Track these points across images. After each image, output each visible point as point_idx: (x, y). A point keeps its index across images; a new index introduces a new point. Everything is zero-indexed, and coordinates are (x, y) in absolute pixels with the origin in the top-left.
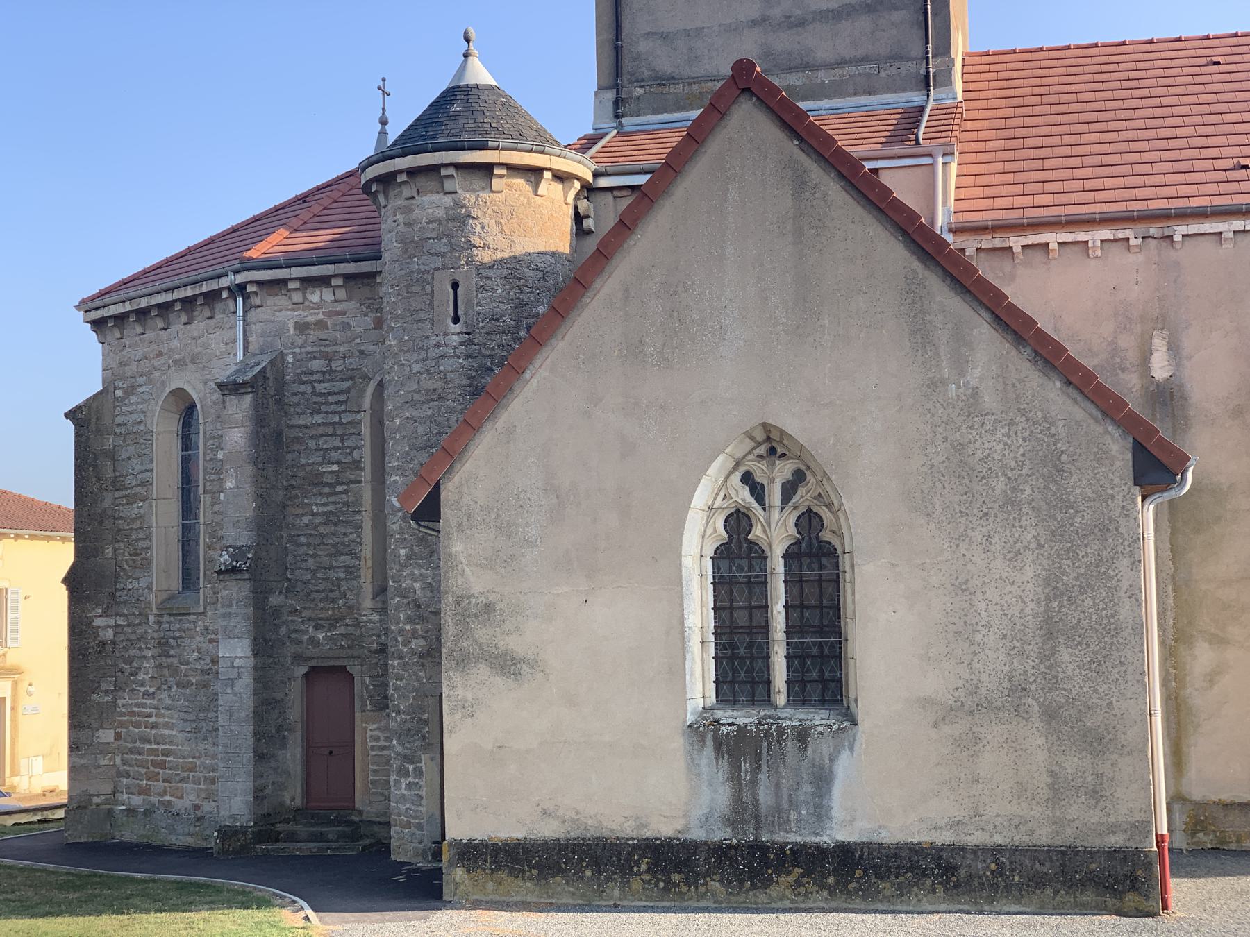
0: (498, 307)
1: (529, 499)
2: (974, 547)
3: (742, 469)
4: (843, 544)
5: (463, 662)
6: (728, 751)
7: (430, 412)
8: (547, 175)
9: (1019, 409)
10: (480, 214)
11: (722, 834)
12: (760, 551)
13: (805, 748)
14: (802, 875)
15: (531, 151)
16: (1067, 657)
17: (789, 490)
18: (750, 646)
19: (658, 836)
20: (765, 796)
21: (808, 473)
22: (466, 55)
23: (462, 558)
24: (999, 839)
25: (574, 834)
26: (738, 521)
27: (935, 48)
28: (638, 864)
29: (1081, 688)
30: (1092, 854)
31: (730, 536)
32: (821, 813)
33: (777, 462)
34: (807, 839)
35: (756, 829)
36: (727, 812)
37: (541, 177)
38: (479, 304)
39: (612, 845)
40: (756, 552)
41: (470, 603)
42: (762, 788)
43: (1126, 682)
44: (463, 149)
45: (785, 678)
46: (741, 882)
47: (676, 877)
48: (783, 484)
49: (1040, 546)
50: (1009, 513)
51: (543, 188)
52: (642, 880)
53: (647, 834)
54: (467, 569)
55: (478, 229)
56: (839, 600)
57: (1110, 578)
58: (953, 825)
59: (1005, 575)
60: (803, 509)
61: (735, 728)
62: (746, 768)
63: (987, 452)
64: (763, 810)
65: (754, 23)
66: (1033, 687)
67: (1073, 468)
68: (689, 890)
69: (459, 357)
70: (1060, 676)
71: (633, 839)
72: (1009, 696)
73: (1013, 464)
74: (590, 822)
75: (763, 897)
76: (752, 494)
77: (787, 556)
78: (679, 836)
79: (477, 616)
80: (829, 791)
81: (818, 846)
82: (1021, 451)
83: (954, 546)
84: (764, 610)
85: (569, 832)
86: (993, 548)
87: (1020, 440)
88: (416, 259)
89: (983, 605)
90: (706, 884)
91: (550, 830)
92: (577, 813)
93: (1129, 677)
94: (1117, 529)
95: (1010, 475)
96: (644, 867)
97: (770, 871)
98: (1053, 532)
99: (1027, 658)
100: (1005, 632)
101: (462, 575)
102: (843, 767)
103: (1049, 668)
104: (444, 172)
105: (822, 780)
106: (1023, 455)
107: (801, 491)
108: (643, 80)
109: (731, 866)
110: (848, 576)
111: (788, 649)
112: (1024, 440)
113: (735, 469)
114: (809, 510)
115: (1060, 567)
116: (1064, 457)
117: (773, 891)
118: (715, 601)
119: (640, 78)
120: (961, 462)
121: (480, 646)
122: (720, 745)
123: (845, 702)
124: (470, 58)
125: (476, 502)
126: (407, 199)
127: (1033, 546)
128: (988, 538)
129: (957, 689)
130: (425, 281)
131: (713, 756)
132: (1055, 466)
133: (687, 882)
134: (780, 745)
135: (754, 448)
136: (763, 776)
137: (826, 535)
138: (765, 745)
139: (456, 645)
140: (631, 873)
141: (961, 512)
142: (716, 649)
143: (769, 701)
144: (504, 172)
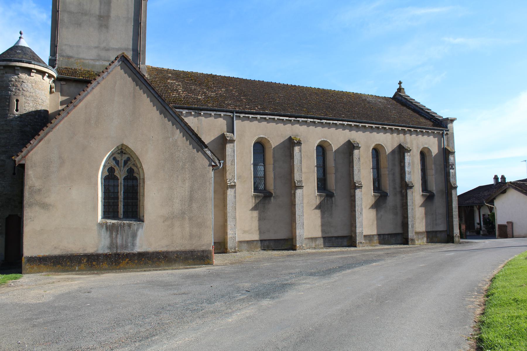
0: (30, 108)
1: (54, 160)
2: (174, 178)
3: (114, 156)
4: (140, 177)
5: (31, 205)
6: (109, 230)
7: (6, 136)
8: (47, 74)
9: (186, 146)
10: (26, 82)
11: (107, 251)
12: (117, 178)
13: (130, 229)
14: (129, 261)
15: (44, 67)
16: (195, 206)
17: (126, 163)
18: (114, 202)
19: (89, 253)
20: (119, 241)
21: (131, 158)
22: (20, 38)
23: (32, 176)
24: (177, 249)
25: (64, 253)
26: (111, 170)
27: (142, 62)
28: (83, 260)
29: (197, 212)
30: (198, 251)
31: (109, 174)
32: (133, 245)
33: (123, 155)
34: (130, 252)
35: (116, 249)
36: (109, 245)
37: (45, 75)
38: (25, 107)
39: (75, 256)
40: (116, 178)
41: (34, 188)
42: (118, 239)
43: (207, 211)
44: (23, 62)
45: (123, 211)
46: (112, 264)
47: (94, 263)
48: (125, 161)
49: (190, 179)
50: (182, 170)
51: (45, 78)
52: (84, 264)
53: (86, 252)
54: (33, 179)
55: (26, 86)
56: (138, 191)
57: (205, 187)
58: (167, 246)
59: (181, 185)
60: (129, 167)
61: (112, 223)
62: (114, 234)
63: (178, 156)
65: (96, 47)
66: (187, 212)
67: (197, 161)
68: (98, 266)
69: (17, 121)
70: (193, 210)
71: (81, 254)
72: (181, 214)
73: (184, 159)
74: (69, 250)
75: (118, 267)
76: (116, 163)
77: (124, 179)
78: (95, 252)
79: (36, 192)
80: (136, 240)
81: (133, 254)
82: (186, 156)
83: (170, 178)
84: (117, 193)
85: (63, 253)
86: (179, 179)
87: (186, 153)
88: (4, 92)
89: (176, 193)
90: (102, 264)
92: (65, 247)
93: (208, 210)
94: (206, 175)
95: (183, 161)
96: (85, 261)
97: (120, 260)
98: (193, 176)
99: (186, 205)
100: (181, 199)
101: (32, 180)
102: (140, 233)
103: (190, 208)
104: (16, 68)
106: (186, 157)
107: (129, 163)
108: (64, 56)
109: (110, 259)
110: (141, 185)
111: (124, 203)
112: (187, 153)
113: (112, 156)
114: (131, 168)
115: (194, 184)
116: (196, 158)
117: (121, 265)
118: (104, 190)
119: (63, 55)
120: (172, 157)
121: (36, 201)
122: (107, 228)
123: (138, 217)
124: (22, 39)
125: (37, 160)
126: (2, 74)
127: (188, 179)
128: (178, 176)
129: (169, 213)
130: (7, 98)
131: (105, 231)
132: (194, 160)
133: (97, 264)
134: (124, 228)
135: (118, 151)
137: (135, 175)
138: (120, 228)
139: (29, 200)
140: (81, 263)
141: (171, 170)
142: (104, 203)
143: (118, 217)
144: (35, 71)
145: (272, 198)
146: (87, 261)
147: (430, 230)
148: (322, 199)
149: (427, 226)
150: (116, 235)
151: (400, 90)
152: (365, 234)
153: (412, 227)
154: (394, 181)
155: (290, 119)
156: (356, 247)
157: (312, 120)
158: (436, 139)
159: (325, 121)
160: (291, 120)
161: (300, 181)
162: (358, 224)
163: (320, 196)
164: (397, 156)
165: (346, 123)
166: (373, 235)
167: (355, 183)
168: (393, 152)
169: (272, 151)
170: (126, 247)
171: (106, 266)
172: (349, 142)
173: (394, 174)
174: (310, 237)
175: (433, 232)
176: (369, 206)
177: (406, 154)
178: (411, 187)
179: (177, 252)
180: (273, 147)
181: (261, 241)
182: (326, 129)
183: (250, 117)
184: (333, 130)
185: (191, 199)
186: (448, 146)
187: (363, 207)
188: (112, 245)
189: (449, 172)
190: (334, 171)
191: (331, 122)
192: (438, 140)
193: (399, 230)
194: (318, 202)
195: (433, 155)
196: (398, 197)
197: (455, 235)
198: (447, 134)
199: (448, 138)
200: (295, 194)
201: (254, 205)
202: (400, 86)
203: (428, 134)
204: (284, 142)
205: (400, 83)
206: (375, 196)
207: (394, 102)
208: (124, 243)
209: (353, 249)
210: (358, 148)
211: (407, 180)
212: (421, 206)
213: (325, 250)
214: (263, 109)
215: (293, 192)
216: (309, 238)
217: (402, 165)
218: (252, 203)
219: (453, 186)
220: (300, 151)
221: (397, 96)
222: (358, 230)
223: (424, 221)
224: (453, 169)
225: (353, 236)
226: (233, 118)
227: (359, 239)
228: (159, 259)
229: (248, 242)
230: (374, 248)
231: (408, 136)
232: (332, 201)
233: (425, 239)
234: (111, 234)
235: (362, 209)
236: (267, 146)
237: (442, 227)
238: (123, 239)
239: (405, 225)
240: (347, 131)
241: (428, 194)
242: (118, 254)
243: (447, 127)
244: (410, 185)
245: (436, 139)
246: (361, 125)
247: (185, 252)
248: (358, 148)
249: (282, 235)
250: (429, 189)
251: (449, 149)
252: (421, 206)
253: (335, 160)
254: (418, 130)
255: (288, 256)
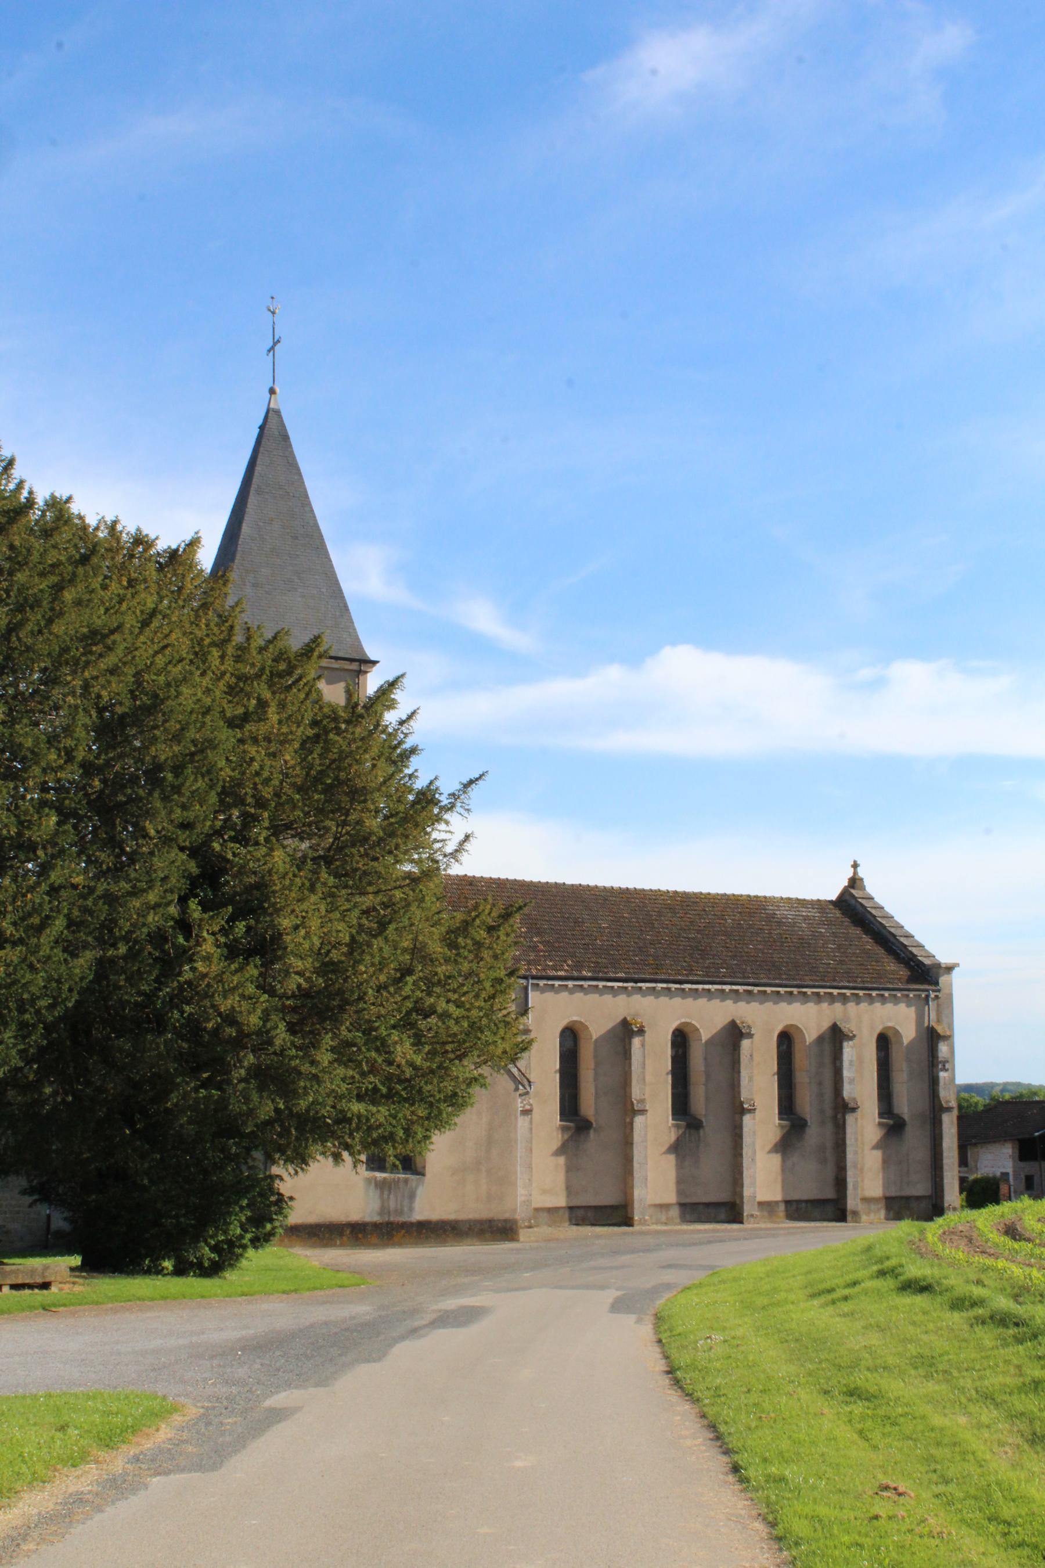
11: (376, 1219)
20: (392, 1204)
24: (471, 1216)
30: (499, 1220)
32: (411, 1209)
47: (360, 1236)
62: (386, 1193)
64: (391, 1209)
91: (312, 1219)
96: (348, 1232)
102: (420, 1192)
105: (412, 1196)
136: (392, 1196)
145: (592, 1132)
146: (352, 1232)
147: (893, 1194)
148: (680, 1132)
149: (886, 1186)
150: (389, 1196)
151: (855, 882)
152: (760, 1198)
153: (855, 1188)
154: (820, 1095)
155: (625, 985)
156: (741, 1222)
157: (664, 985)
158: (913, 1009)
159: (689, 986)
160: (626, 988)
161: (642, 1101)
162: (747, 1181)
163: (677, 1126)
164: (827, 1048)
165: (727, 988)
166: (777, 1203)
167: (742, 1103)
168: (820, 1039)
169: (592, 1047)
170: (401, 1212)
171: (374, 1240)
172: (733, 1024)
173: (820, 1083)
174: (658, 1202)
175: (901, 1198)
176: (769, 1147)
177: (845, 1044)
178: (854, 1110)
179: (469, 1221)
180: (594, 1037)
181: (571, 1208)
182: (690, 1000)
183: (556, 985)
184: (702, 1001)
185: (490, 1141)
186: (939, 1021)
187: (757, 1147)
188: (383, 1210)
189: (938, 1077)
190: (703, 1079)
191: (700, 987)
192: (917, 1009)
193: (829, 1193)
194: (672, 1137)
195: (906, 1041)
196: (829, 1129)
197: (946, 1205)
198: (937, 997)
199: (938, 1005)
200: (632, 1124)
201: (560, 1144)
202: (855, 873)
203: (896, 1000)
204: (614, 1029)
205: (855, 866)
206: (781, 1126)
207: (838, 913)
208: (399, 1207)
209: (735, 1226)
210: (750, 1036)
211: (846, 1094)
212: (876, 1147)
213: (685, 1227)
214: (578, 966)
215: (628, 1120)
216: (655, 1205)
217: (838, 1064)
218: (556, 1139)
219: (945, 1105)
220: (643, 1045)
221: (847, 897)
222: (747, 1192)
223: (881, 1176)
224: (947, 1070)
225: (738, 1202)
226: (526, 988)
227: (747, 1210)
228: (445, 1231)
229: (552, 1211)
230: (776, 1226)
231: (851, 1006)
232: (699, 1137)
233: (883, 1213)
234: (382, 1193)
235: (755, 1153)
236: (582, 1035)
237: (921, 1188)
238: (397, 1200)
239: (840, 1183)
240: (729, 1003)
241: (891, 1122)
242: (392, 1223)
243: (937, 983)
244: (852, 1105)
245: (913, 1009)
246: (756, 989)
247: (481, 1222)
248: (750, 1036)
249: (607, 1197)
250: (896, 1111)
251: (940, 1029)
252: (876, 1147)
253: (706, 1059)
254: (874, 993)
255: (625, 1234)
